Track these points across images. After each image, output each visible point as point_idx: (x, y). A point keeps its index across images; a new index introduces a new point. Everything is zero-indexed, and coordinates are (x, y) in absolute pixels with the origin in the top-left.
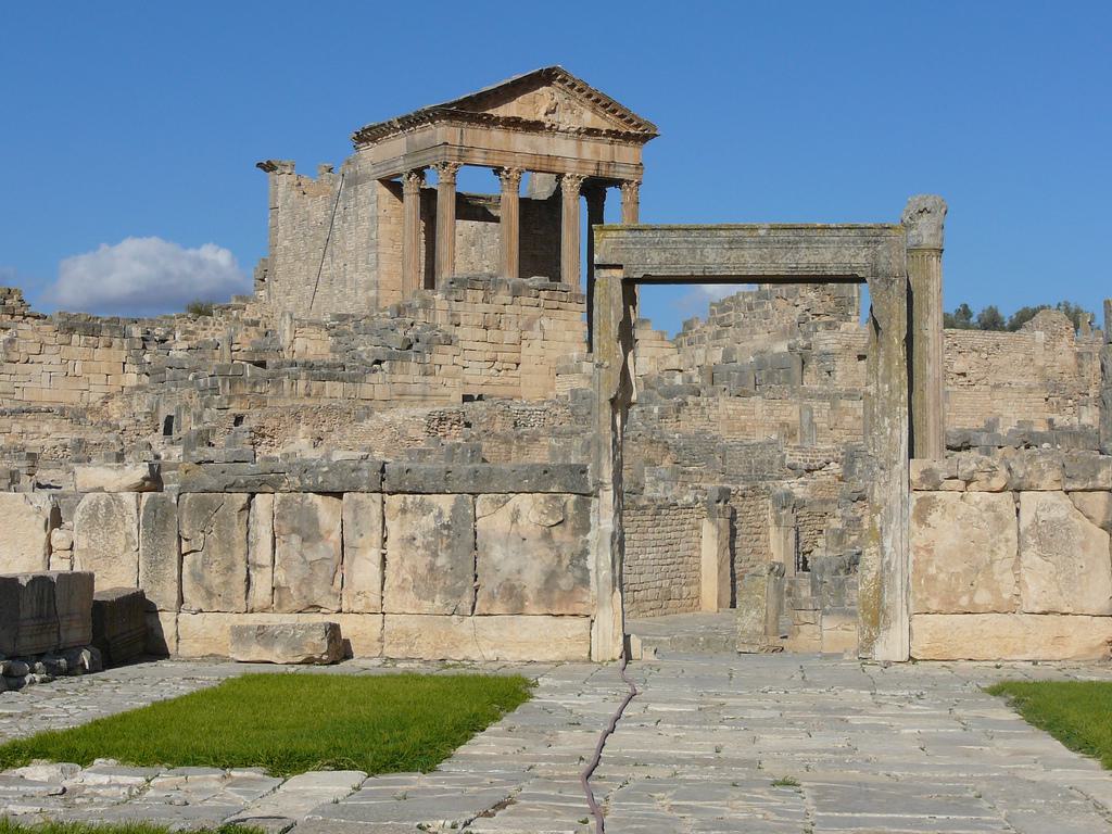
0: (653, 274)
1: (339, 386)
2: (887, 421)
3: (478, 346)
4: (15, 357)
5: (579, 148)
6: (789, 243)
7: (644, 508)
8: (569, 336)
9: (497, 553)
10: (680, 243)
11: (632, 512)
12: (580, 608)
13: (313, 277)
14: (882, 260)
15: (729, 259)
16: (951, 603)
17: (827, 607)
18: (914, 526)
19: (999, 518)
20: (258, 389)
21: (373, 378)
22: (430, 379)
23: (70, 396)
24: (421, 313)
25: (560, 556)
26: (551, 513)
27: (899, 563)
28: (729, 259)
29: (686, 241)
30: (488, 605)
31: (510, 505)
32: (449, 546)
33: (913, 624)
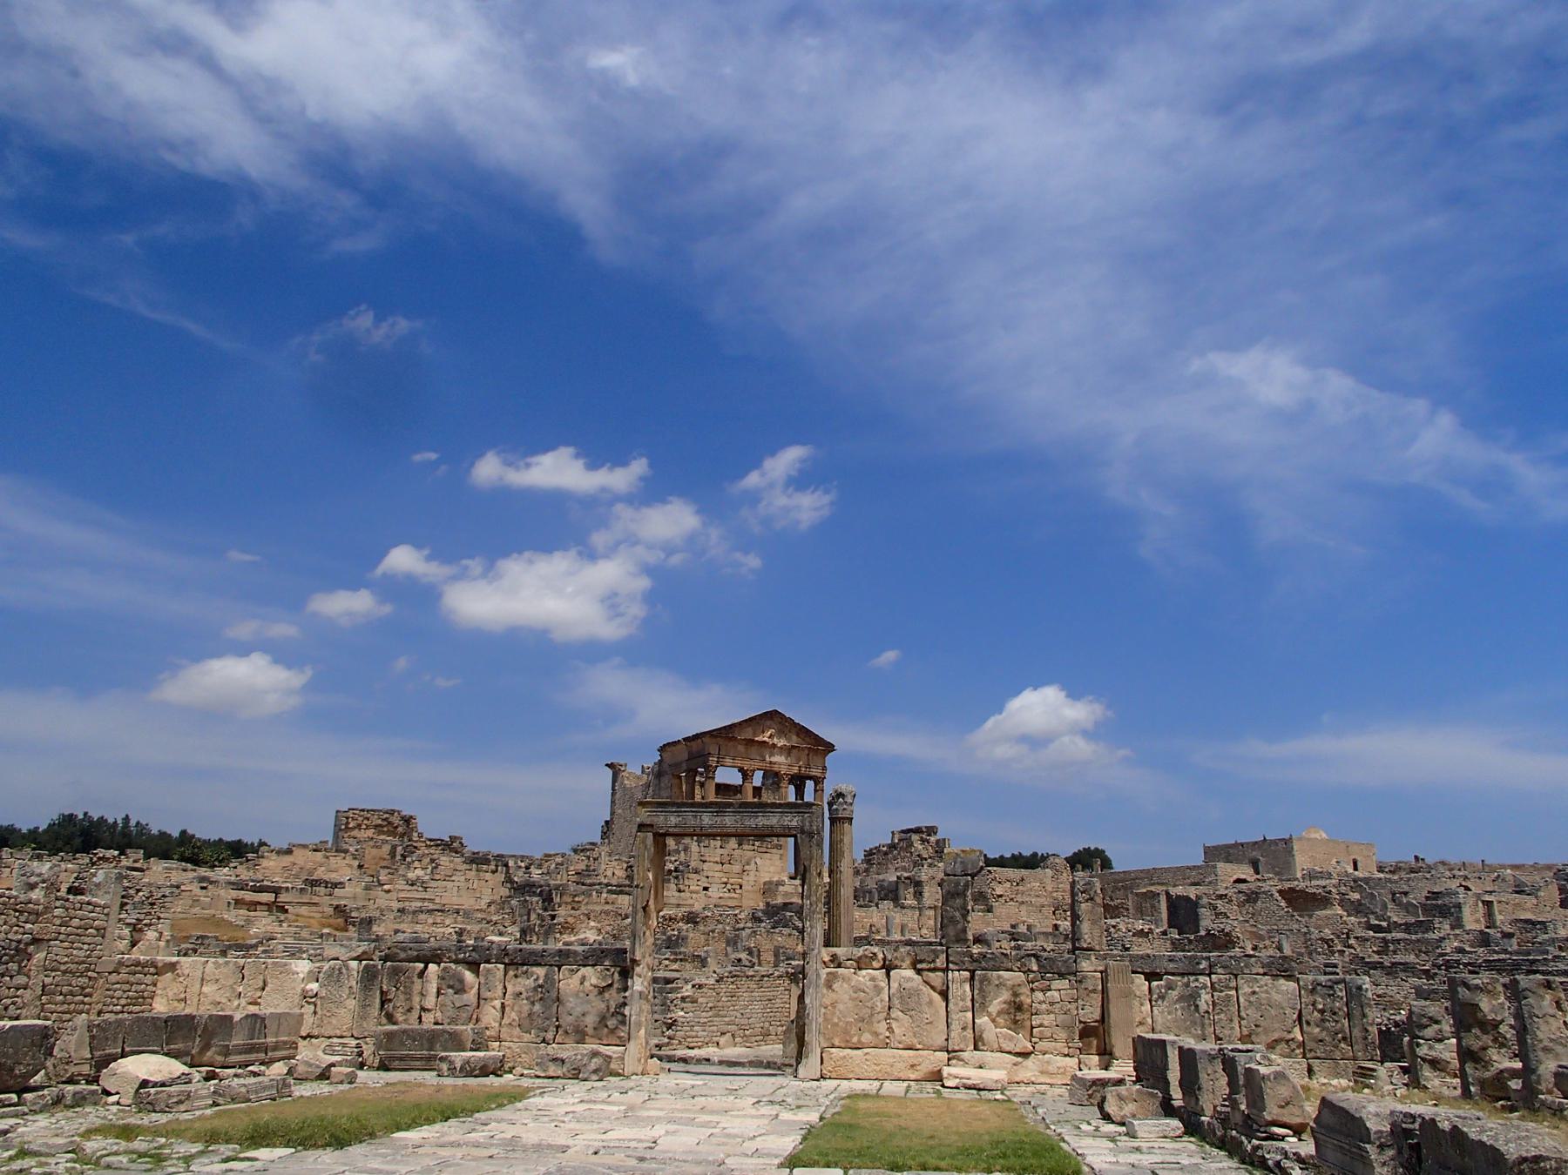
3: (717, 874)
4: (437, 877)
7: (752, 976)
8: (772, 869)
9: (569, 1005)
10: (688, 812)
11: (744, 979)
14: (807, 824)
16: (847, 1041)
18: (825, 991)
20: (577, 899)
23: (467, 902)
26: (604, 979)
31: (580, 973)
32: (541, 999)
33: (824, 1055)
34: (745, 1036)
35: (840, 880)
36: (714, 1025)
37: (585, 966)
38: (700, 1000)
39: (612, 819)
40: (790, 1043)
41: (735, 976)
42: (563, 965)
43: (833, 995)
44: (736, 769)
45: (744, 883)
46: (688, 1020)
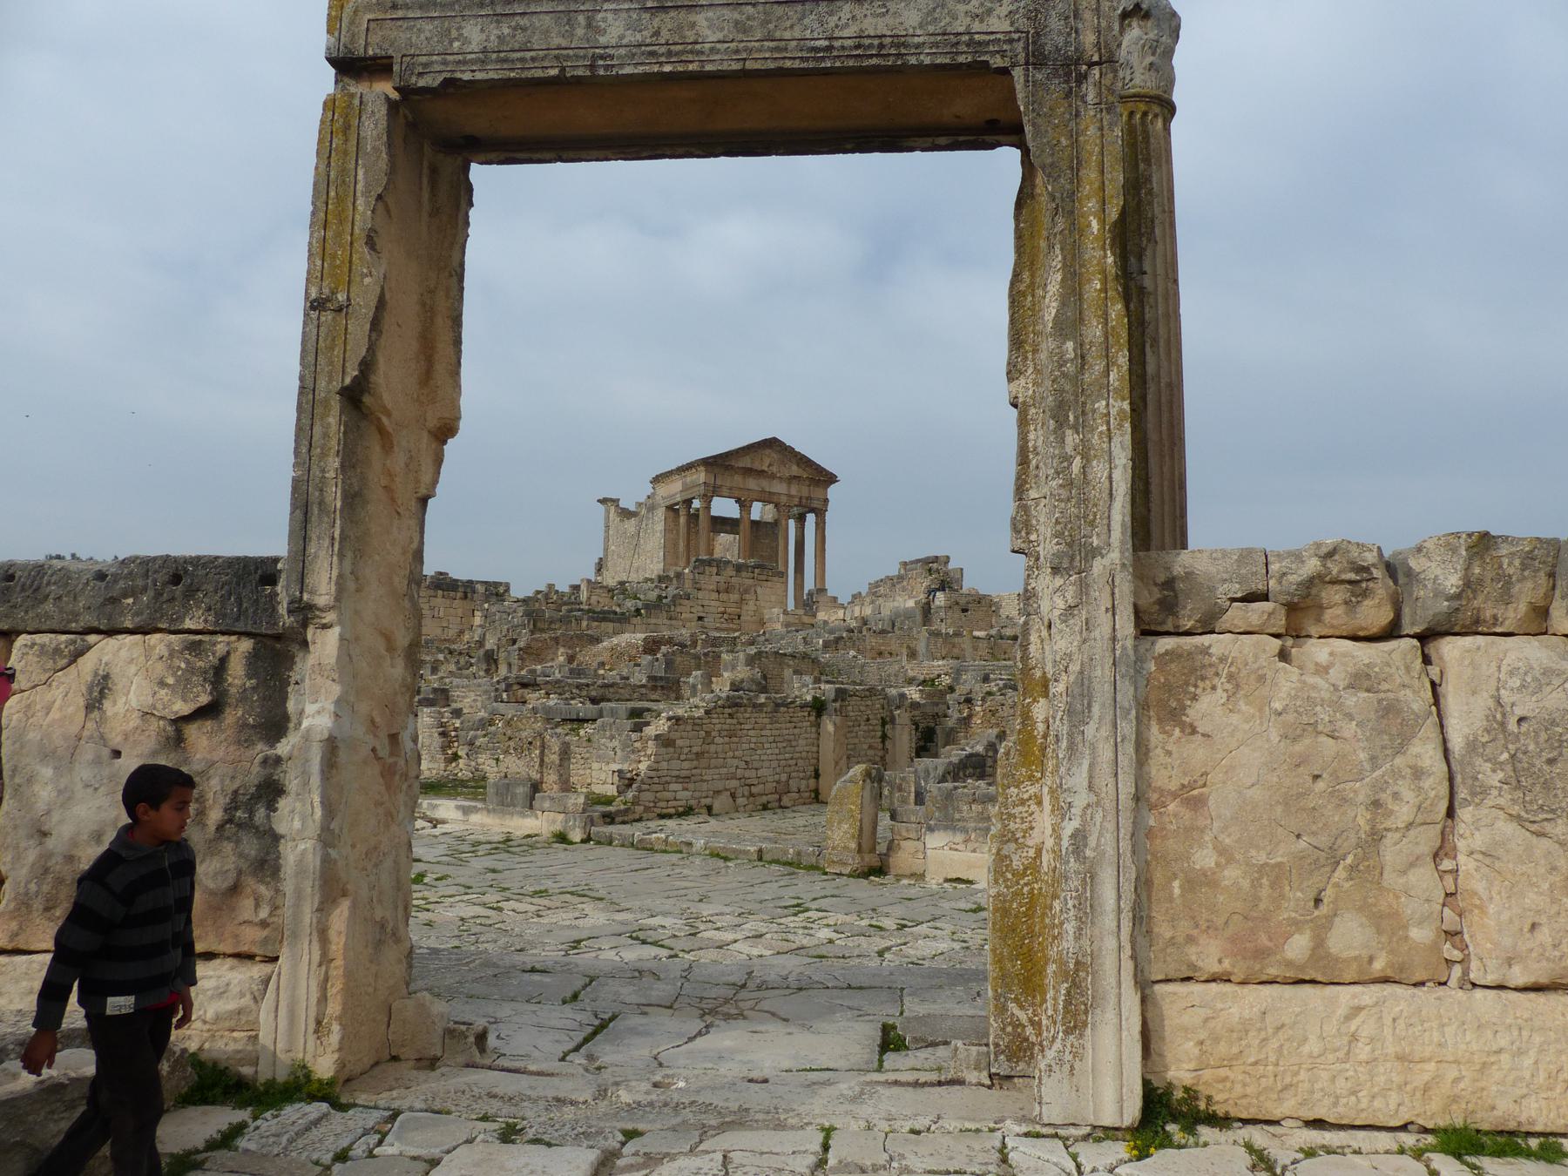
0: (467, 76)
1: (611, 625)
2: (1071, 438)
3: (713, 603)
5: (789, 488)
8: (773, 598)
11: (749, 709)
12: (250, 938)
14: (1055, 23)
15: (657, 33)
16: (1261, 954)
17: (932, 822)
19: (1389, 710)
20: (553, 626)
22: (673, 622)
24: (675, 581)
26: (183, 687)
27: (1109, 837)
28: (657, 33)
30: (14, 925)
31: (88, 663)
34: (752, 795)
36: (702, 781)
37: (111, 632)
38: (679, 743)
40: (839, 823)
41: (737, 705)
42: (19, 633)
43: (1196, 753)
45: (743, 613)
46: (660, 773)
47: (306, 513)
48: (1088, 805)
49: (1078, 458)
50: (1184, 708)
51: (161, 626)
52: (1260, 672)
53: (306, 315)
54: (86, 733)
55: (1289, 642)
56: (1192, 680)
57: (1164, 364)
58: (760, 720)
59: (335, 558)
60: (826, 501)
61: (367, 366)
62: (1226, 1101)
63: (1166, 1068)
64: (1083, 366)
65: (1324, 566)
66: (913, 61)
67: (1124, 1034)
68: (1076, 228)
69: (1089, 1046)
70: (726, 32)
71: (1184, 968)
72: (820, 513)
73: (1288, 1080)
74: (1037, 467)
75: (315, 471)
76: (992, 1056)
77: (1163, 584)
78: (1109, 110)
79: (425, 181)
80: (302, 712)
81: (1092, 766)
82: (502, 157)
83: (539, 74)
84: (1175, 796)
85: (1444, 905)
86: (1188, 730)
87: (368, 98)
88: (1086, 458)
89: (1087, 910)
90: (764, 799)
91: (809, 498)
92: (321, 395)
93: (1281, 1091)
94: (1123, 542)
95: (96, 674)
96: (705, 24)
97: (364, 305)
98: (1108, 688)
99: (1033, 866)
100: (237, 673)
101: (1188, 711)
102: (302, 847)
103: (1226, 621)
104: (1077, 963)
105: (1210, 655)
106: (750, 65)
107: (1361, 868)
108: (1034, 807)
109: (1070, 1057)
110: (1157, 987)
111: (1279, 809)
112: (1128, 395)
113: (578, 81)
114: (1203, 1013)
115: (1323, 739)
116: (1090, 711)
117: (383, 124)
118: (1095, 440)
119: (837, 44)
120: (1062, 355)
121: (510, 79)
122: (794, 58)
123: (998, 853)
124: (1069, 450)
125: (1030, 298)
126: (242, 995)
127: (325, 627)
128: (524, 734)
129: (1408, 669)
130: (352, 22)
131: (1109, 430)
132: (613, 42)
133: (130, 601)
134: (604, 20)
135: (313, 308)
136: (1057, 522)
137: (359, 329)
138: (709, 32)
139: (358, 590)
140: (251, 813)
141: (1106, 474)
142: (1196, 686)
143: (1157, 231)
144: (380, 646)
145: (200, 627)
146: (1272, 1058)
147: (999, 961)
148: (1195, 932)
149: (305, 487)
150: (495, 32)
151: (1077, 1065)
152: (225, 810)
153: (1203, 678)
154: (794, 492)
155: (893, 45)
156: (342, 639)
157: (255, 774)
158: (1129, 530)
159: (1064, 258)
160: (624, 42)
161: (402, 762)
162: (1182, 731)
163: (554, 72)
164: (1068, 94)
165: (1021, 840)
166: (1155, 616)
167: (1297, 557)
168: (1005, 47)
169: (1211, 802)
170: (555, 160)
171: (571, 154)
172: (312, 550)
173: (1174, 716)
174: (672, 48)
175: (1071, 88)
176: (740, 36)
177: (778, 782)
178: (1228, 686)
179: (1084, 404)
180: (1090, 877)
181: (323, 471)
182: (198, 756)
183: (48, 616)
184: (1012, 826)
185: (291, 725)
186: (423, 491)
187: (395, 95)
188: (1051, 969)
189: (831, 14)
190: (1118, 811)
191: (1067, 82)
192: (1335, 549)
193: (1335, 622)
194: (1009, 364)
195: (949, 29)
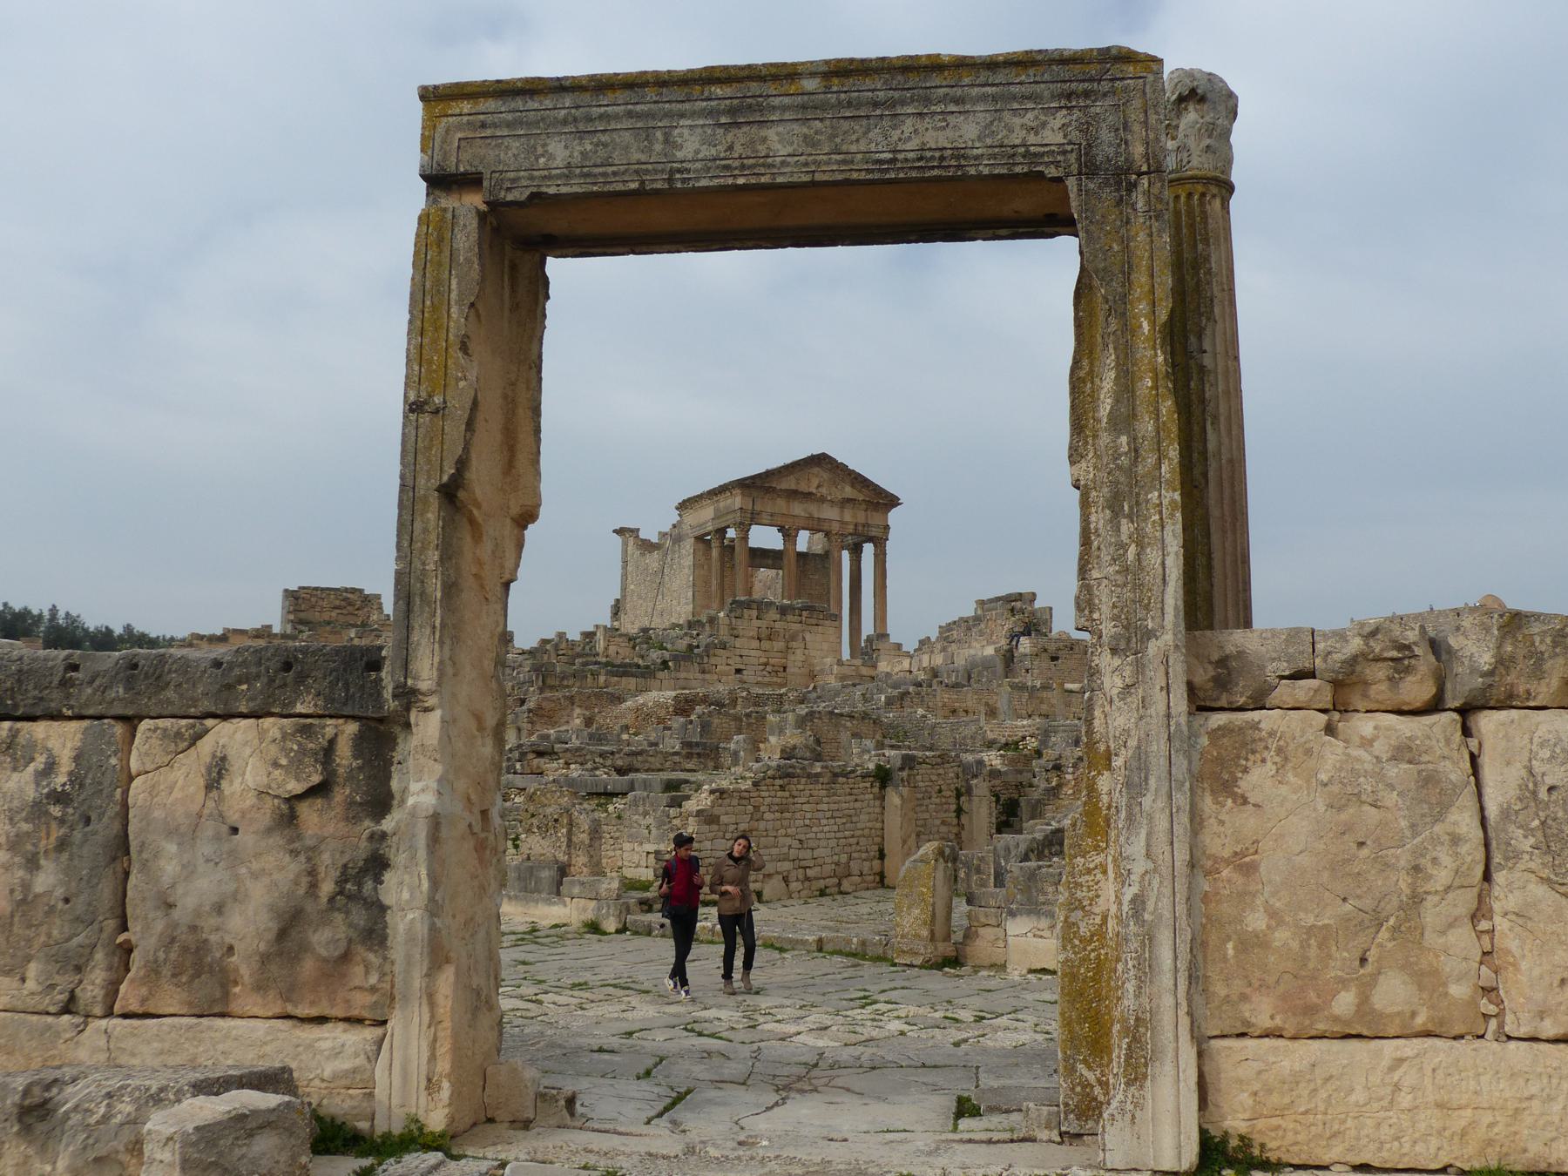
0: (552, 191)
1: (633, 680)
2: (1126, 527)
3: (753, 653)
6: (876, 105)
8: (825, 646)
10: (617, 117)
11: (803, 780)
12: (361, 1003)
13: (650, 610)
14: (1105, 135)
15: (730, 148)
16: (1310, 1010)
17: (1013, 906)
19: (1428, 780)
20: (565, 683)
21: (660, 675)
22: (707, 676)
24: (707, 627)
25: (312, 872)
26: (295, 768)
27: (1165, 903)
28: (730, 148)
29: (630, 114)
30: (144, 991)
31: (206, 746)
32: (62, 845)
34: (807, 879)
35: (1203, 401)
37: (226, 717)
38: (724, 819)
39: (624, 596)
42: (141, 718)
43: (1247, 821)
44: (775, 529)
45: (790, 664)
47: (409, 604)
48: (1146, 872)
49: (1133, 545)
50: (1236, 780)
51: (273, 710)
52: (1307, 746)
53: (405, 417)
54: (206, 811)
55: (1336, 715)
56: (1244, 753)
57: (1225, 440)
58: (815, 793)
59: (437, 646)
60: (887, 527)
61: (462, 464)
62: (1279, 1148)
63: (1224, 1118)
64: (1136, 458)
65: (1367, 645)
66: (972, 171)
67: (1182, 1084)
68: (1128, 329)
69: (1149, 1096)
70: (795, 146)
71: (1238, 1024)
72: (880, 543)
73: (1336, 1127)
74: (1099, 548)
75: (417, 564)
76: (1062, 1115)
77: (1217, 662)
78: (1157, 218)
79: (506, 278)
80: (405, 790)
81: (1149, 835)
82: (578, 251)
83: (620, 187)
84: (1228, 862)
85: (1481, 963)
86: (1240, 801)
87: (461, 212)
88: (1141, 546)
89: (1146, 970)
90: (822, 884)
91: (866, 525)
92: (421, 492)
93: (1330, 1138)
94: (1176, 625)
95: (214, 756)
96: (776, 138)
97: (459, 407)
98: (1163, 762)
99: (1099, 933)
100: (344, 755)
101: (1240, 783)
102: (410, 916)
103: (1273, 698)
104: (1137, 1019)
105: (1259, 730)
106: (819, 177)
107: (1403, 929)
108: (1099, 876)
109: (1131, 1107)
110: (1213, 1042)
111: (1326, 874)
112: (1179, 487)
113: (657, 192)
114: (1256, 1065)
115: (1366, 808)
116: (1147, 784)
117: (474, 236)
118: (1149, 529)
119: (900, 156)
120: (1116, 448)
121: (593, 193)
122: (860, 170)
123: (1066, 921)
124: (1124, 538)
125: (1089, 385)
126: (356, 1055)
127: (427, 710)
128: (549, 810)
129: (1448, 741)
130: (444, 141)
131: (1161, 519)
132: (690, 157)
133: (245, 687)
134: (681, 135)
135: (412, 411)
136: (1114, 606)
137: (454, 430)
138: (779, 147)
139: (455, 675)
140: (360, 885)
141: (1159, 561)
142: (1247, 759)
143: (1217, 310)
144: (473, 726)
145: (311, 711)
146: (1322, 1107)
147: (1068, 1024)
148: (1248, 991)
149: (407, 580)
150: (578, 148)
151: (1138, 1114)
152: (337, 883)
153: (1254, 752)
154: (848, 517)
155: (953, 157)
156: (443, 721)
157: (363, 848)
158: (1182, 614)
159: (1117, 357)
160: (700, 156)
161: (492, 837)
162: (1234, 802)
163: (634, 186)
164: (1120, 202)
165: (1087, 908)
166: (1210, 693)
167: (1341, 636)
168: (1059, 158)
169: (1262, 869)
170: (628, 254)
171: (645, 249)
172: (415, 638)
173: (1226, 787)
174: (745, 161)
175: (1122, 196)
176: (809, 150)
177: (837, 864)
178: (1277, 759)
179: (1138, 494)
180: (1149, 939)
181: (424, 564)
182: (310, 832)
183: (169, 702)
184: (1079, 894)
185: (395, 802)
186: (507, 576)
187: (483, 207)
188: (1117, 1027)
189: (894, 127)
190: (1174, 877)
191: (1118, 190)
192: (1377, 629)
193: (1380, 698)
194: (1070, 448)
195: (1006, 142)
